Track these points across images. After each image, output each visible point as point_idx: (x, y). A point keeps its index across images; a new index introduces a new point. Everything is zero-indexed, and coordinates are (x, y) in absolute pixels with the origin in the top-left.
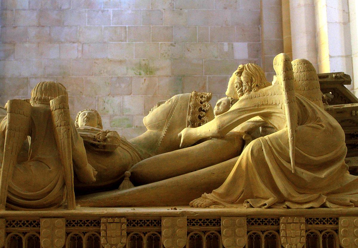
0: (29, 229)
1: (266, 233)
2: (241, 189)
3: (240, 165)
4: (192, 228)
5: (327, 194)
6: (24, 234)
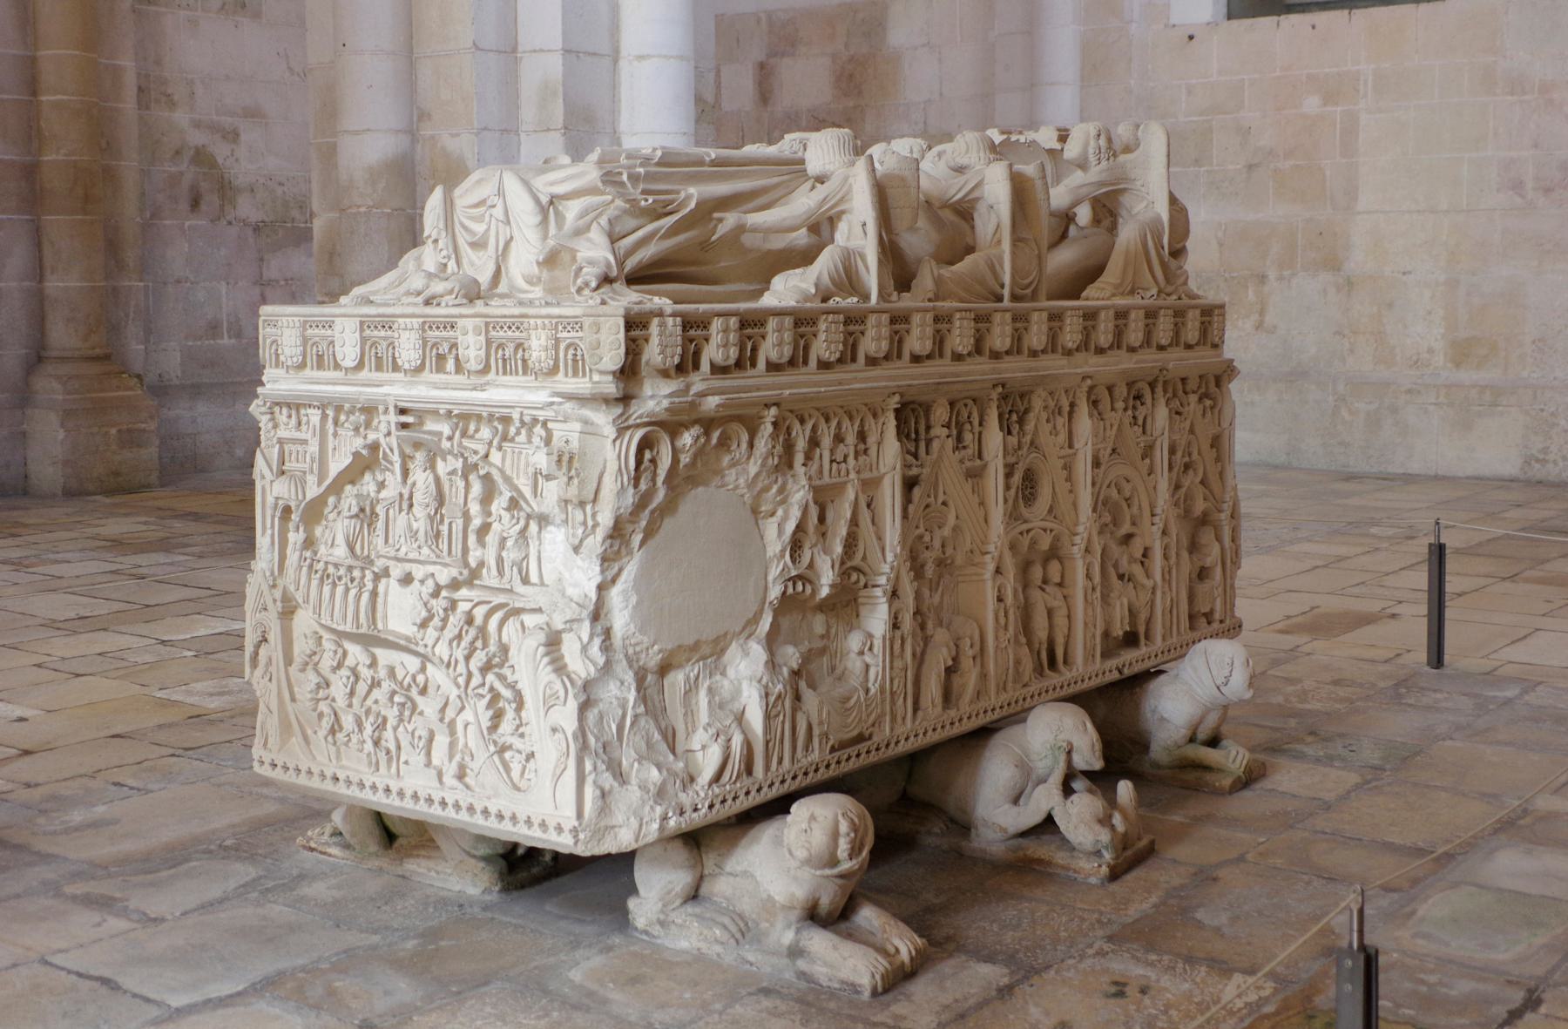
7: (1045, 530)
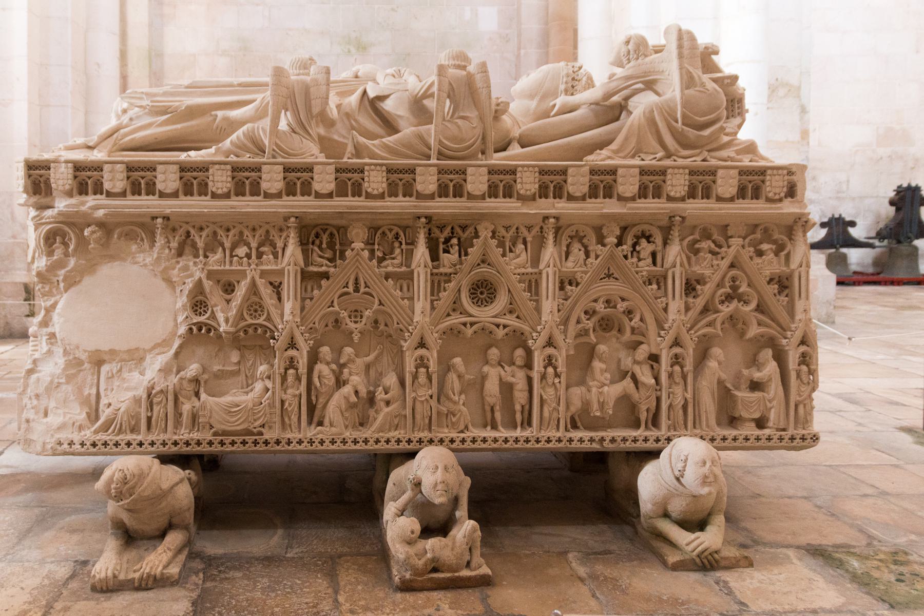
0: (456, 176)
1: (653, 183)
2: (633, 145)
3: (632, 125)
4: (593, 177)
5: (709, 151)
6: (451, 181)
7: (498, 326)
